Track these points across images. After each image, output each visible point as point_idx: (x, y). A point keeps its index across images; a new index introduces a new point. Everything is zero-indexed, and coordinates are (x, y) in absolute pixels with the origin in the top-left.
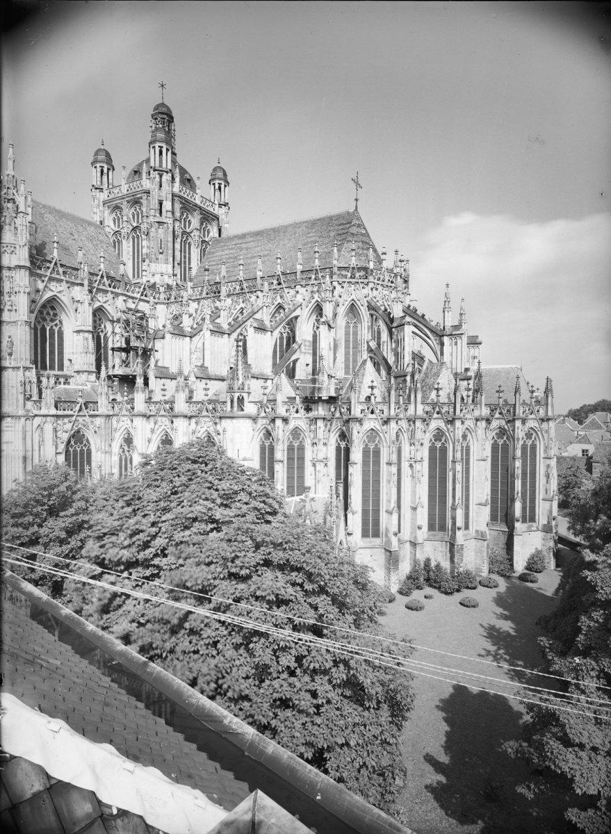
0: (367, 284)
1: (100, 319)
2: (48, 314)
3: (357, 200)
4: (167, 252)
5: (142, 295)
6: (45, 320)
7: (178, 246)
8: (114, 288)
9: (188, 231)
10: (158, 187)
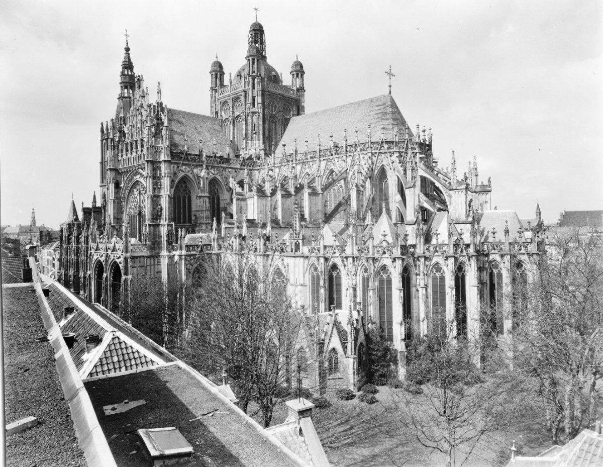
0: (393, 153)
1: (214, 186)
2: (182, 186)
3: (390, 86)
4: (259, 132)
5: (241, 166)
6: (179, 191)
7: (267, 126)
8: (223, 163)
9: (274, 113)
10: (251, 88)
